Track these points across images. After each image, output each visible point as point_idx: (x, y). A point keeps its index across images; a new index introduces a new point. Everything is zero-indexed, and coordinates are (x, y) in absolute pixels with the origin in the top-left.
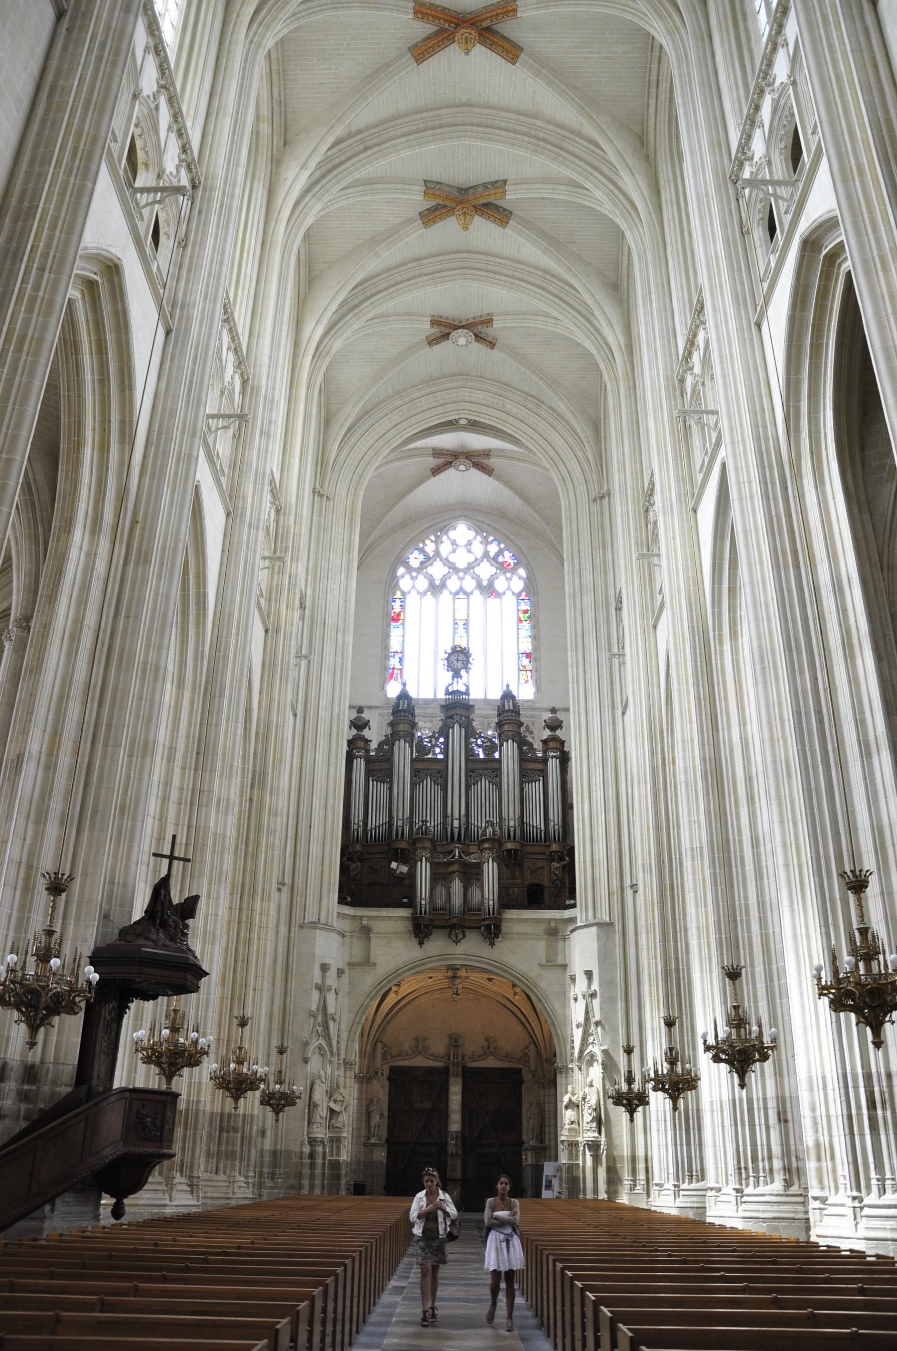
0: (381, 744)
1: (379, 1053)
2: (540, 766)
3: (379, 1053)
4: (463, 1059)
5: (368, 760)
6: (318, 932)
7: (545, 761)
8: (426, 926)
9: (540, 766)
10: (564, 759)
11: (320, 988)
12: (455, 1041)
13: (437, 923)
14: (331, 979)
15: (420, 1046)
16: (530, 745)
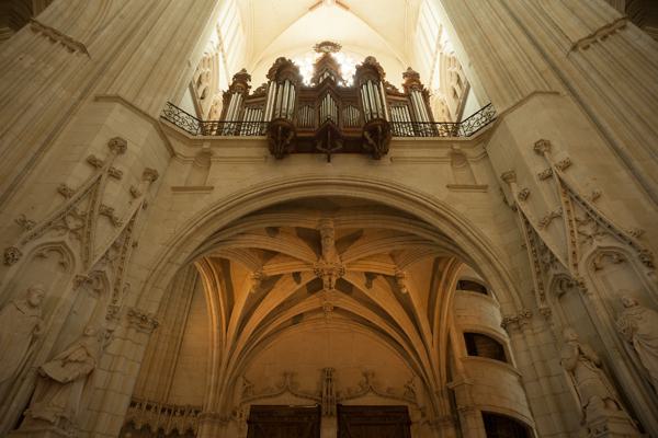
0: (259, 89)
1: (240, 388)
2: (405, 99)
3: (240, 388)
4: (338, 395)
5: (245, 96)
6: (118, 106)
7: (408, 95)
8: (286, 130)
9: (405, 99)
10: (426, 95)
11: (93, 163)
12: (328, 375)
13: (299, 135)
14: (127, 164)
15: (288, 382)
16: (394, 88)
